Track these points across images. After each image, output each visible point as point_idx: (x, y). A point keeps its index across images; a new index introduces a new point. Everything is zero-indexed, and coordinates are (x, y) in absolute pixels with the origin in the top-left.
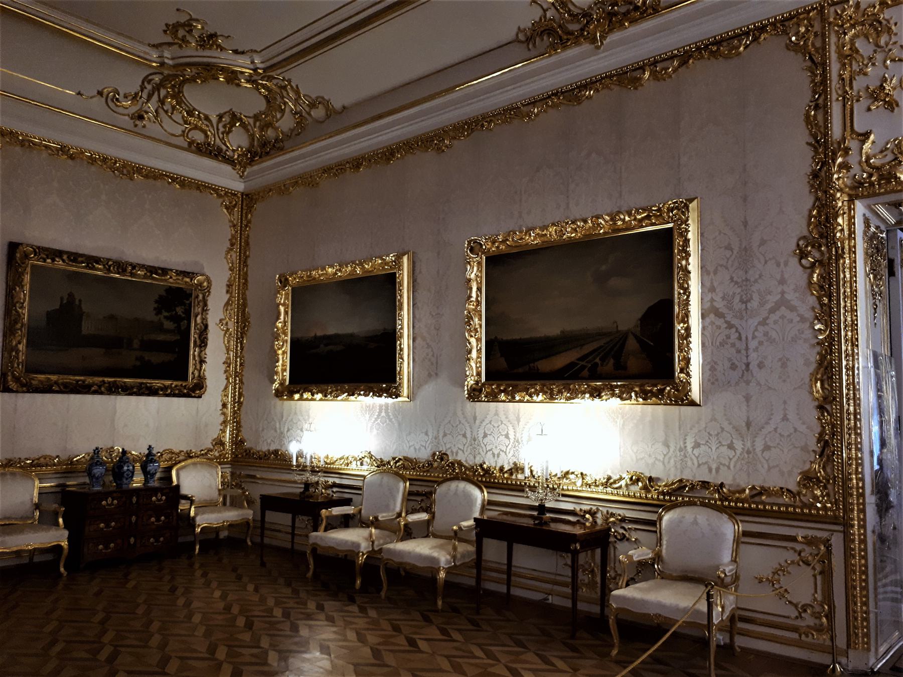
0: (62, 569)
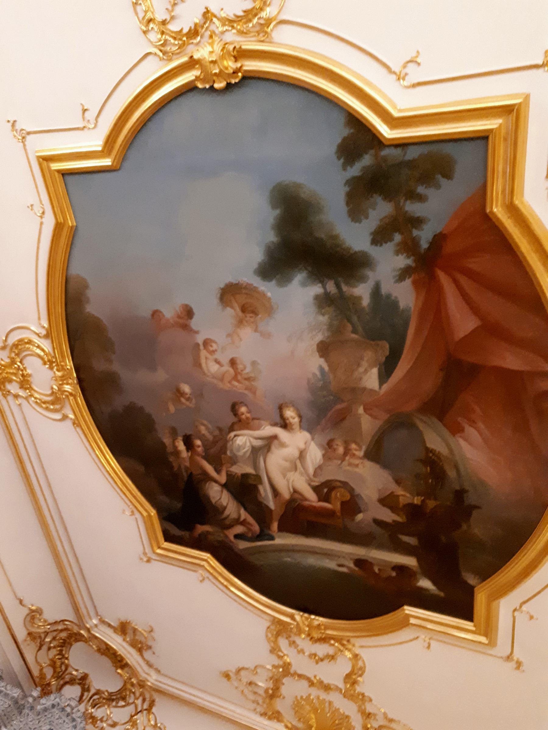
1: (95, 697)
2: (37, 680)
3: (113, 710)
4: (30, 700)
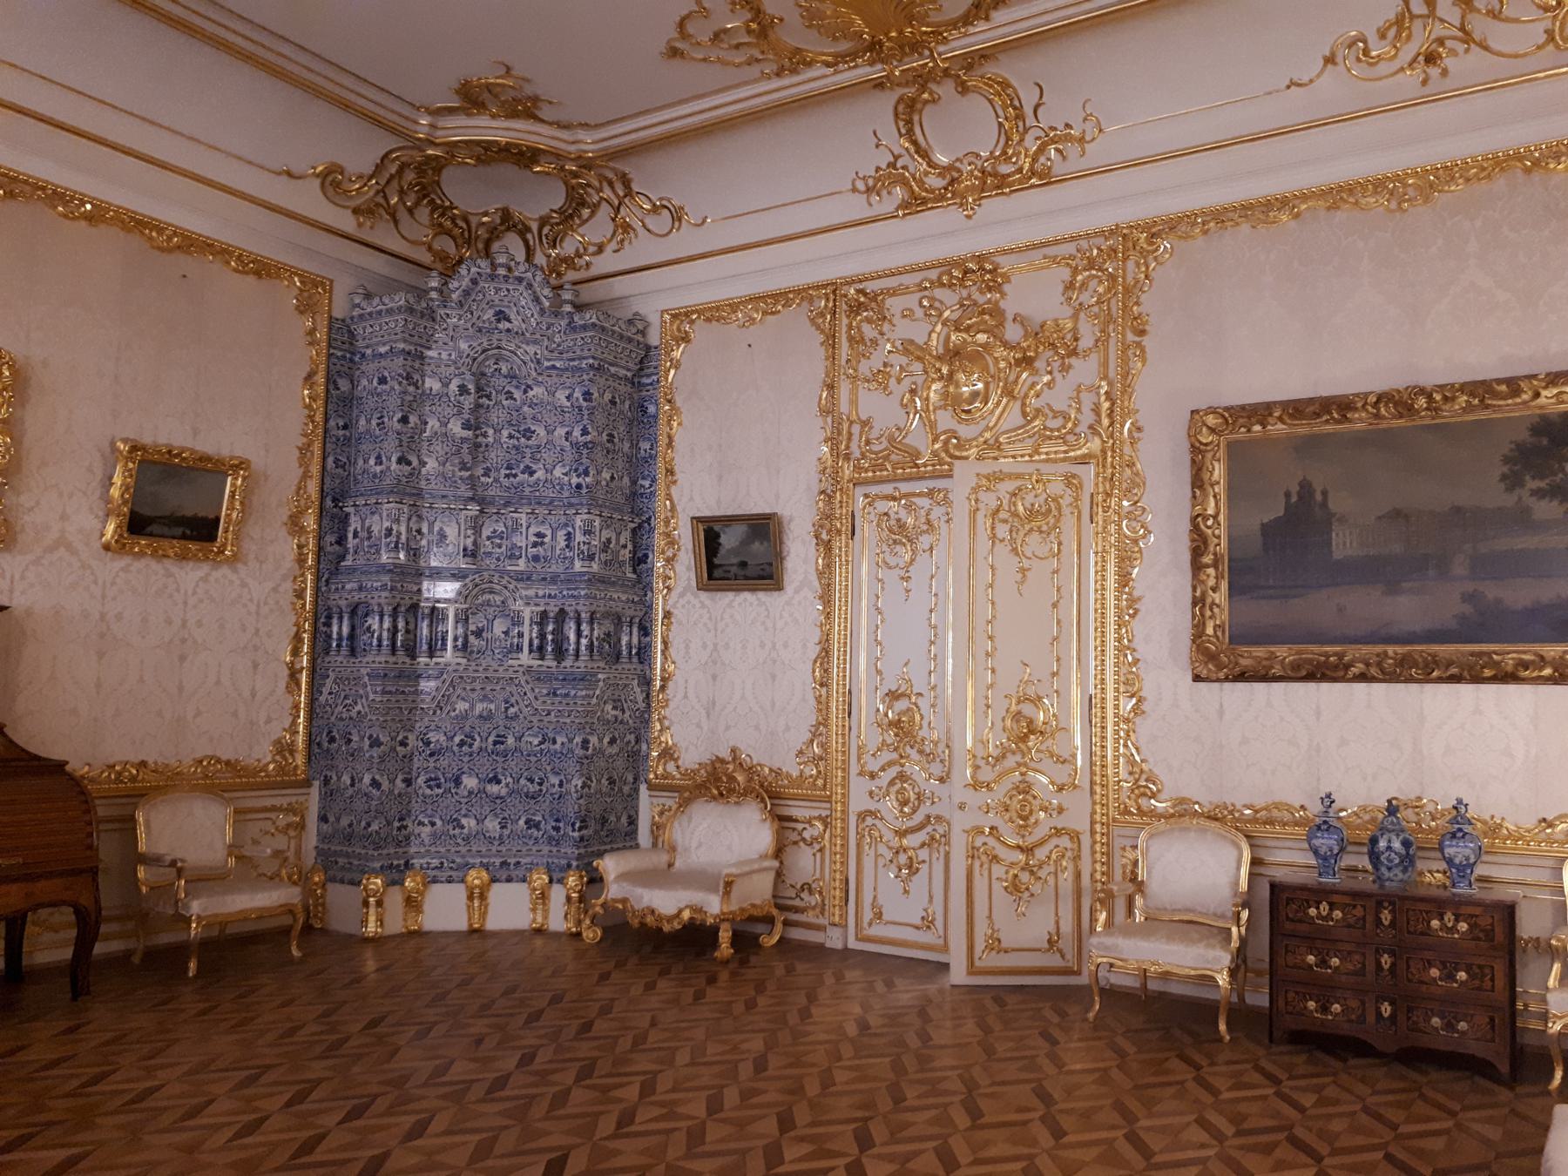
0: (1222, 1027)
1: (546, 230)
3: (580, 230)
4: (434, 295)
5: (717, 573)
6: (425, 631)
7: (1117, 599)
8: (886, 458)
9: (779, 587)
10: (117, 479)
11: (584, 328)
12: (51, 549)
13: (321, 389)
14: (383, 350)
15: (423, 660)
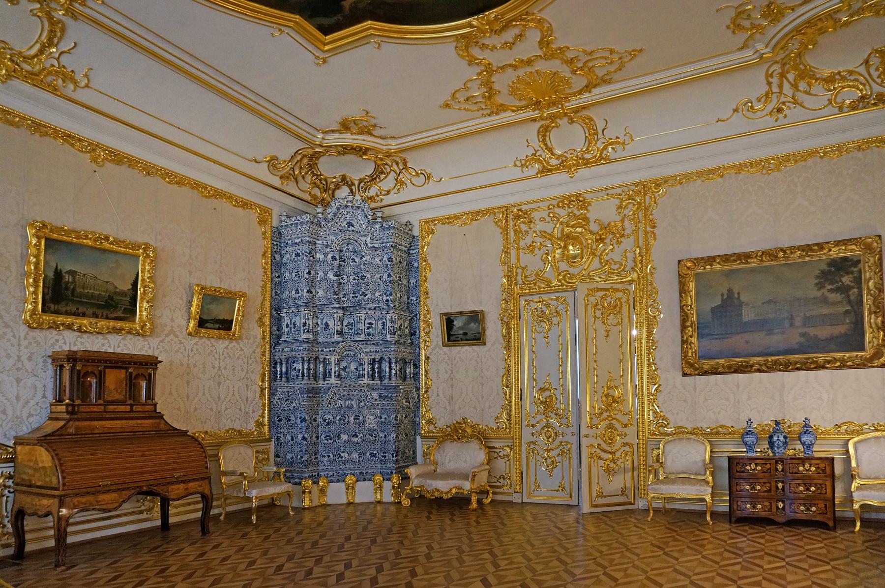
1: (362, 185)
2: (313, 202)
4: (320, 215)
5: (452, 338)
6: (321, 369)
7: (648, 342)
8: (535, 284)
9: (484, 344)
10: (195, 303)
11: (389, 228)
12: (167, 335)
13: (269, 260)
14: (297, 241)
15: (321, 382)
